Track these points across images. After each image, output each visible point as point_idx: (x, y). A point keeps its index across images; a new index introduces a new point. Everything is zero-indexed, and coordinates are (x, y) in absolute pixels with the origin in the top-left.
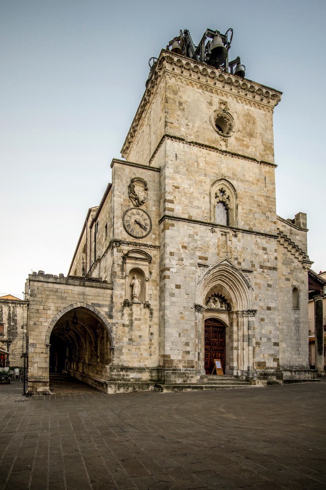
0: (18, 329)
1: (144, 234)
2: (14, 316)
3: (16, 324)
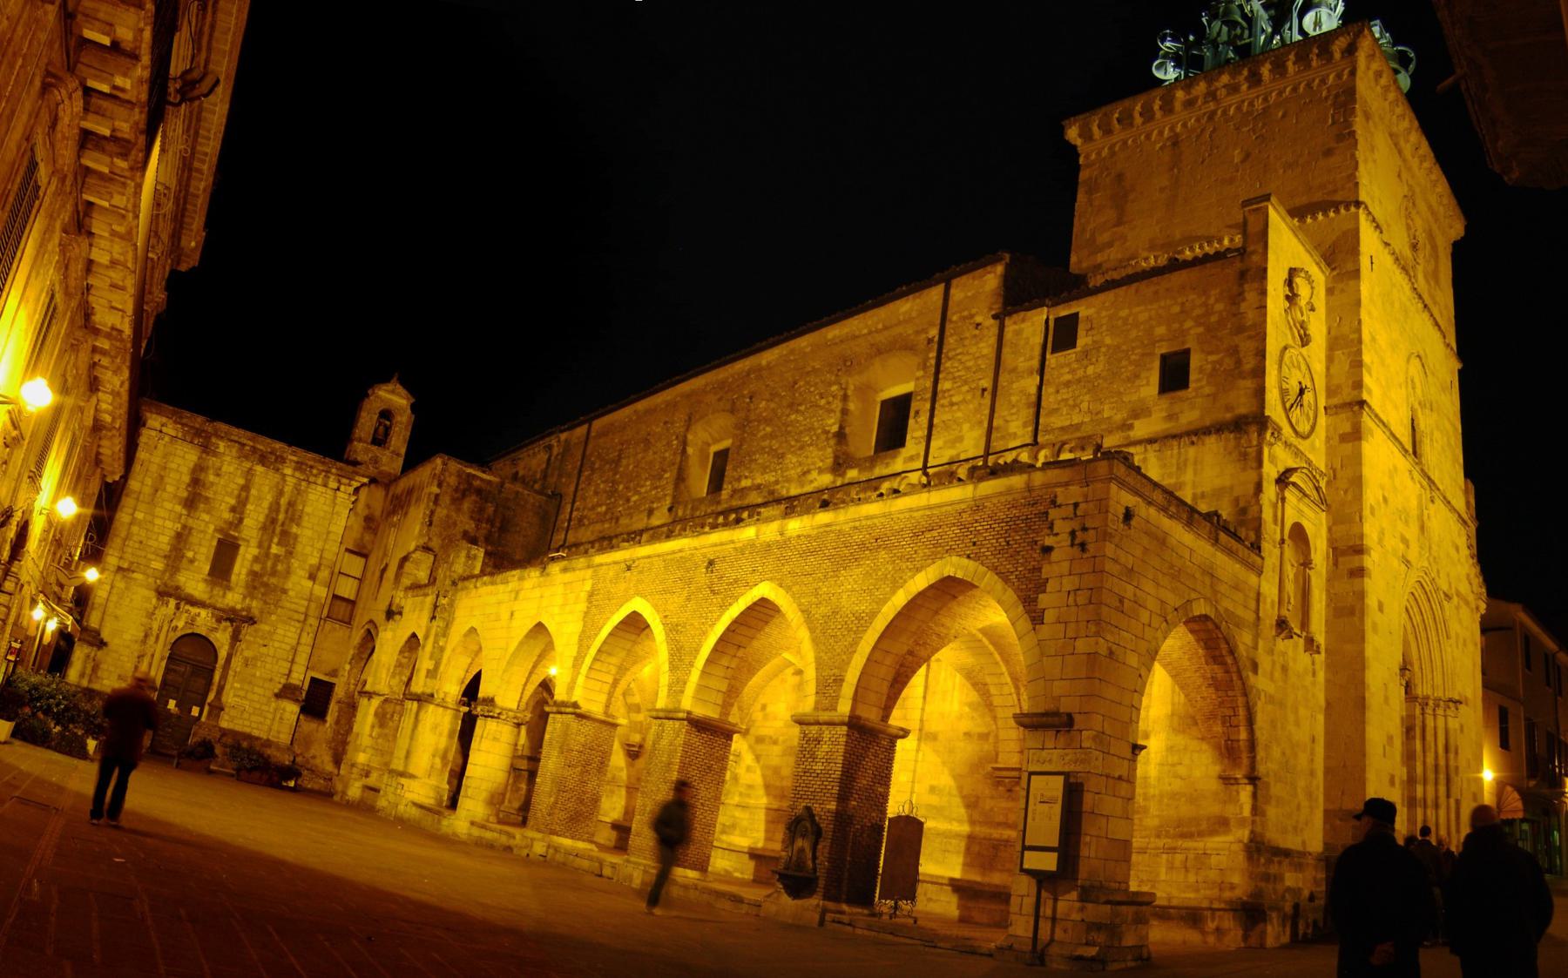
0: (294, 579)
2: (292, 520)
3: (290, 553)
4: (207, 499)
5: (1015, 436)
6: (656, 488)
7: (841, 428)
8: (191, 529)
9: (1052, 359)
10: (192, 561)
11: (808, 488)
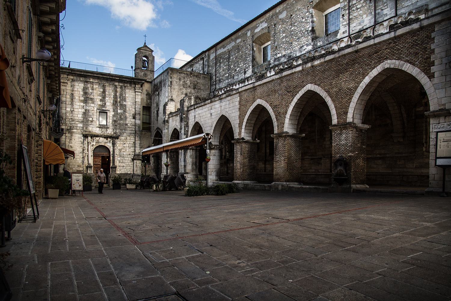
0: (128, 119)
2: (122, 100)
3: (125, 111)
5: (386, 15)
6: (245, 64)
7: (313, 28)
8: (89, 110)
10: (92, 121)
11: (304, 52)
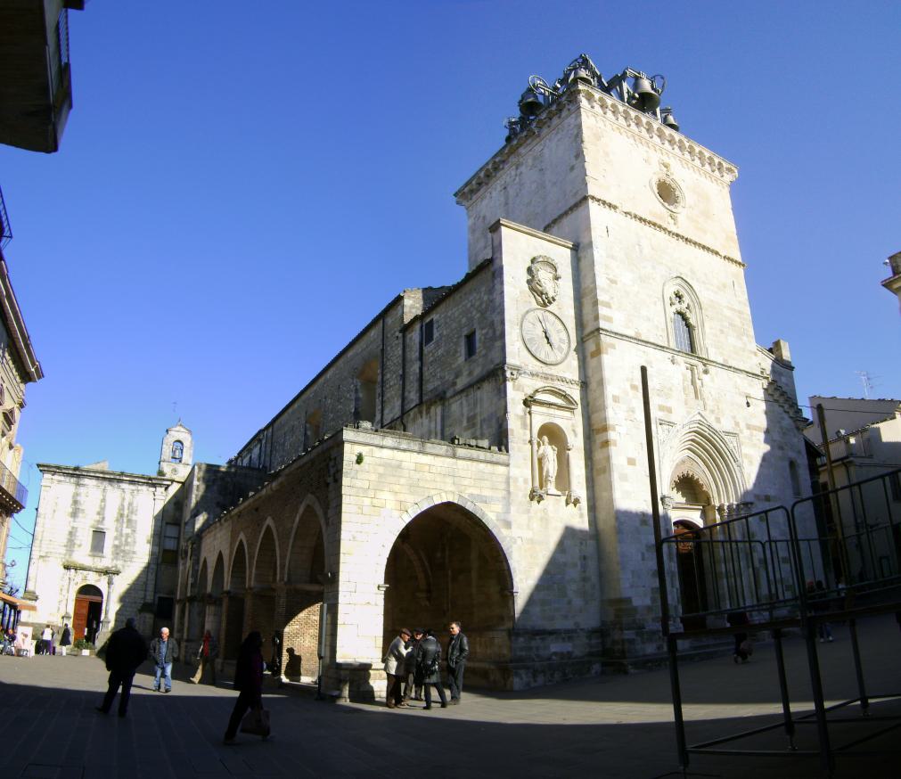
1: (559, 359)
2: (132, 513)
4: (83, 510)
9: (426, 350)
